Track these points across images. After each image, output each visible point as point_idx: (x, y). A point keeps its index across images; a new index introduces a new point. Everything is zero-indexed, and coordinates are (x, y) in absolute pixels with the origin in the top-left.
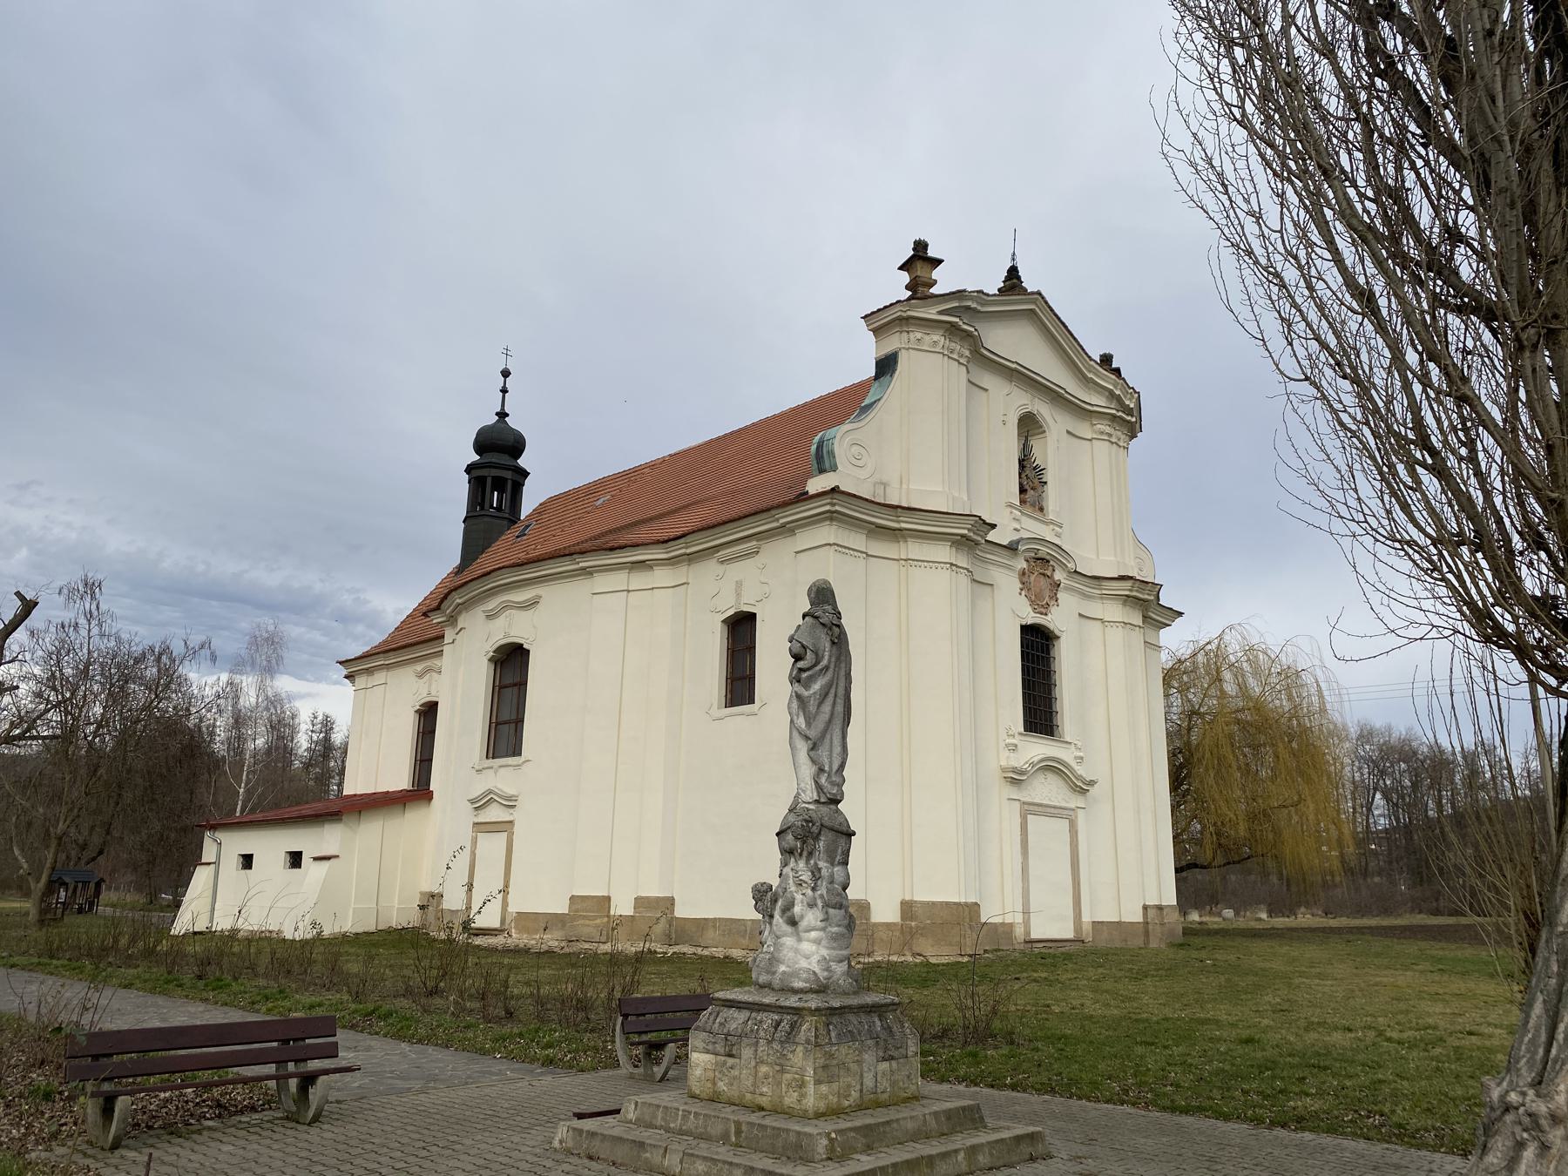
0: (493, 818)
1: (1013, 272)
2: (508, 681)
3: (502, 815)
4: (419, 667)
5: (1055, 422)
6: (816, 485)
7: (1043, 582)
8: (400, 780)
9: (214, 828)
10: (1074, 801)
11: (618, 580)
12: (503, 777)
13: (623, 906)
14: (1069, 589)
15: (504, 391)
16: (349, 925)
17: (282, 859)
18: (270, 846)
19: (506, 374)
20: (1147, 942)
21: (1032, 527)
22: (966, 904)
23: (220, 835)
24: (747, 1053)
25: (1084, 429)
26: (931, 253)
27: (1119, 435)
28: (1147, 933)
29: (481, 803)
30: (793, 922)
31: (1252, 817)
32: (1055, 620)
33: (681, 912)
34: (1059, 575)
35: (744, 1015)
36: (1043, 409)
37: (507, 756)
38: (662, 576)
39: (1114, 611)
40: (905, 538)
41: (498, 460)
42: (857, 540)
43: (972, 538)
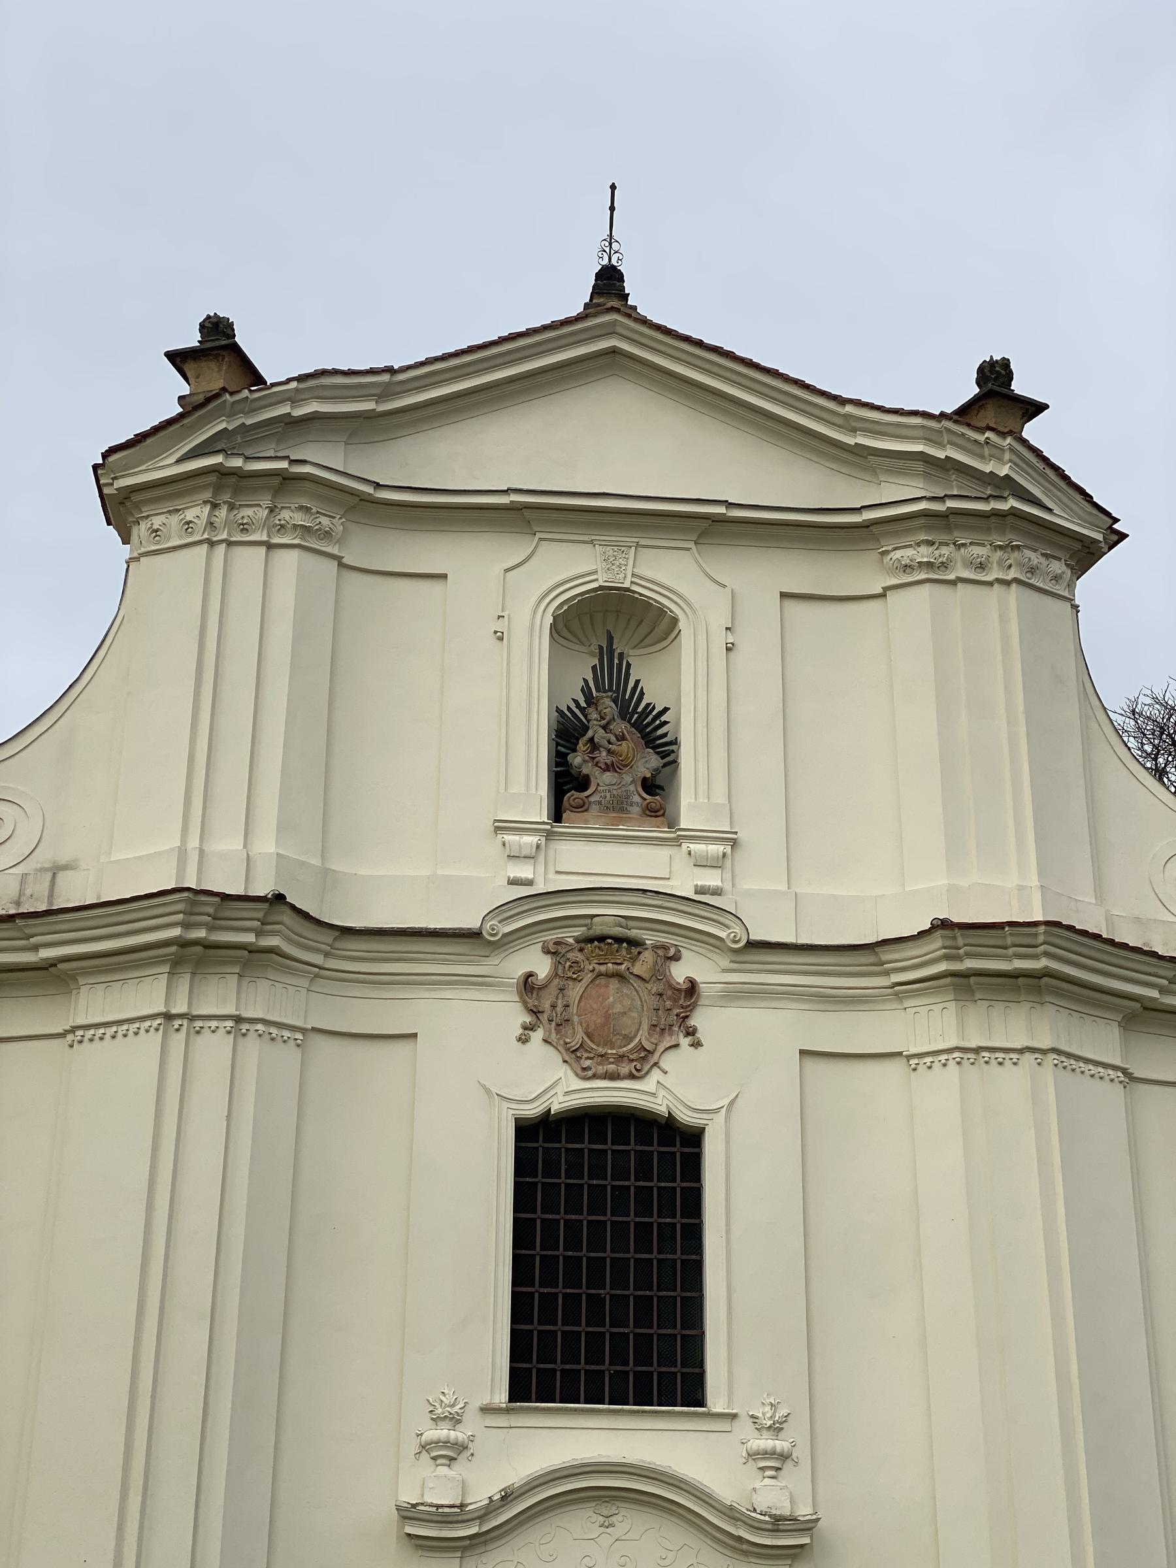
1: (609, 281)
14: (735, 995)
21: (604, 860)
25: (859, 573)
32: (671, 1087)
39: (934, 1024)
43: (230, 938)
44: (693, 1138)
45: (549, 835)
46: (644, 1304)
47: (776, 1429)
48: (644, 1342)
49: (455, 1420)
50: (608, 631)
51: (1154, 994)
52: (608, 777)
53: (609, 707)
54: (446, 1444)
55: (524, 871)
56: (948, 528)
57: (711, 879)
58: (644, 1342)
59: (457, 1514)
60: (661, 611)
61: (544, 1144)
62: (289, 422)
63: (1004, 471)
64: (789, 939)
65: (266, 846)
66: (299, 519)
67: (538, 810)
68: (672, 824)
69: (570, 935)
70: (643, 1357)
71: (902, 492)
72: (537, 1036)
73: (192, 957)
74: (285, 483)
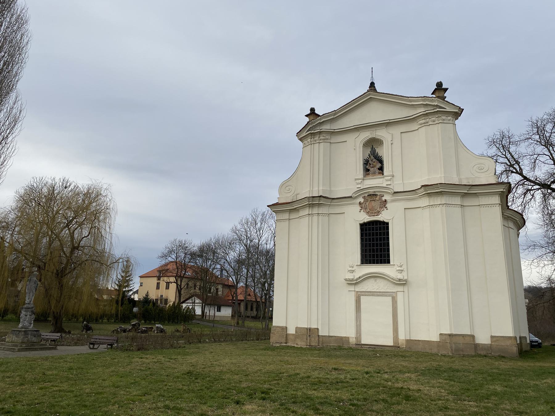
1: (372, 85)
14: (393, 201)
22: (310, 329)
25: (414, 126)
32: (382, 217)
39: (425, 202)
43: (316, 202)
44: (387, 224)
45: (363, 180)
46: (381, 249)
47: (401, 266)
48: (381, 255)
49: (353, 267)
50: (373, 144)
51: (466, 191)
52: (372, 169)
53: (372, 157)
54: (400, 270)
55: (359, 186)
56: (428, 116)
57: (389, 183)
58: (381, 255)
59: (352, 280)
60: (381, 140)
61: (365, 228)
62: (320, 123)
63: (436, 104)
64: (402, 190)
65: (321, 188)
66: (323, 138)
67: (361, 176)
68: (383, 174)
69: (366, 195)
70: (381, 257)
71: (421, 110)
72: (362, 211)
73: (311, 206)
74: (320, 133)
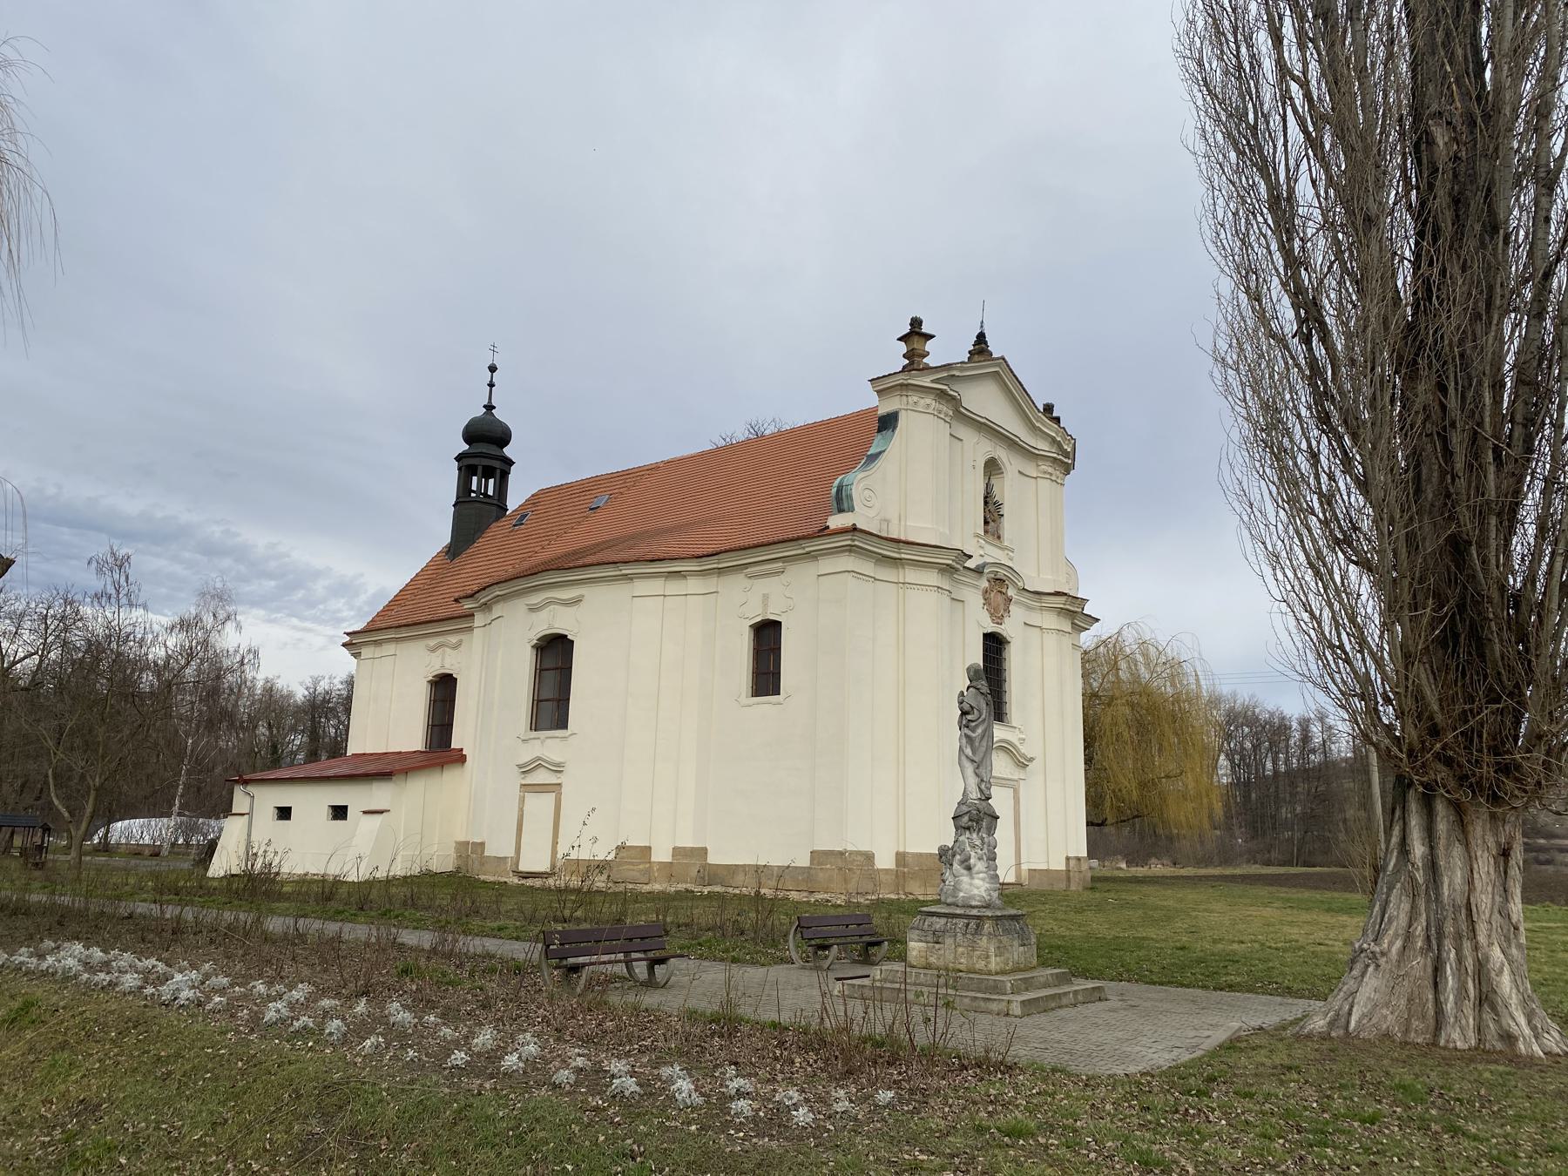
0: (540, 781)
1: (981, 338)
2: (549, 664)
3: (552, 779)
4: (432, 642)
5: (1011, 463)
6: (836, 521)
7: (1000, 598)
8: (411, 736)
9: (246, 782)
10: (1016, 774)
11: (656, 586)
12: (550, 745)
13: (662, 855)
14: (1018, 603)
15: (491, 385)
16: (399, 870)
17: (325, 812)
18: (311, 802)
19: (493, 369)
20: (1068, 886)
23: (251, 789)
24: (949, 941)
25: (1031, 469)
26: (925, 329)
27: (1058, 474)
28: (1069, 879)
29: (526, 769)
30: (969, 868)
31: (1143, 785)
32: (1008, 629)
33: (713, 859)
34: (1011, 592)
35: (943, 921)
36: (1002, 454)
37: (551, 729)
38: (693, 585)
39: (1051, 621)
40: (903, 566)
41: (486, 449)
42: (867, 567)
43: (953, 565)
